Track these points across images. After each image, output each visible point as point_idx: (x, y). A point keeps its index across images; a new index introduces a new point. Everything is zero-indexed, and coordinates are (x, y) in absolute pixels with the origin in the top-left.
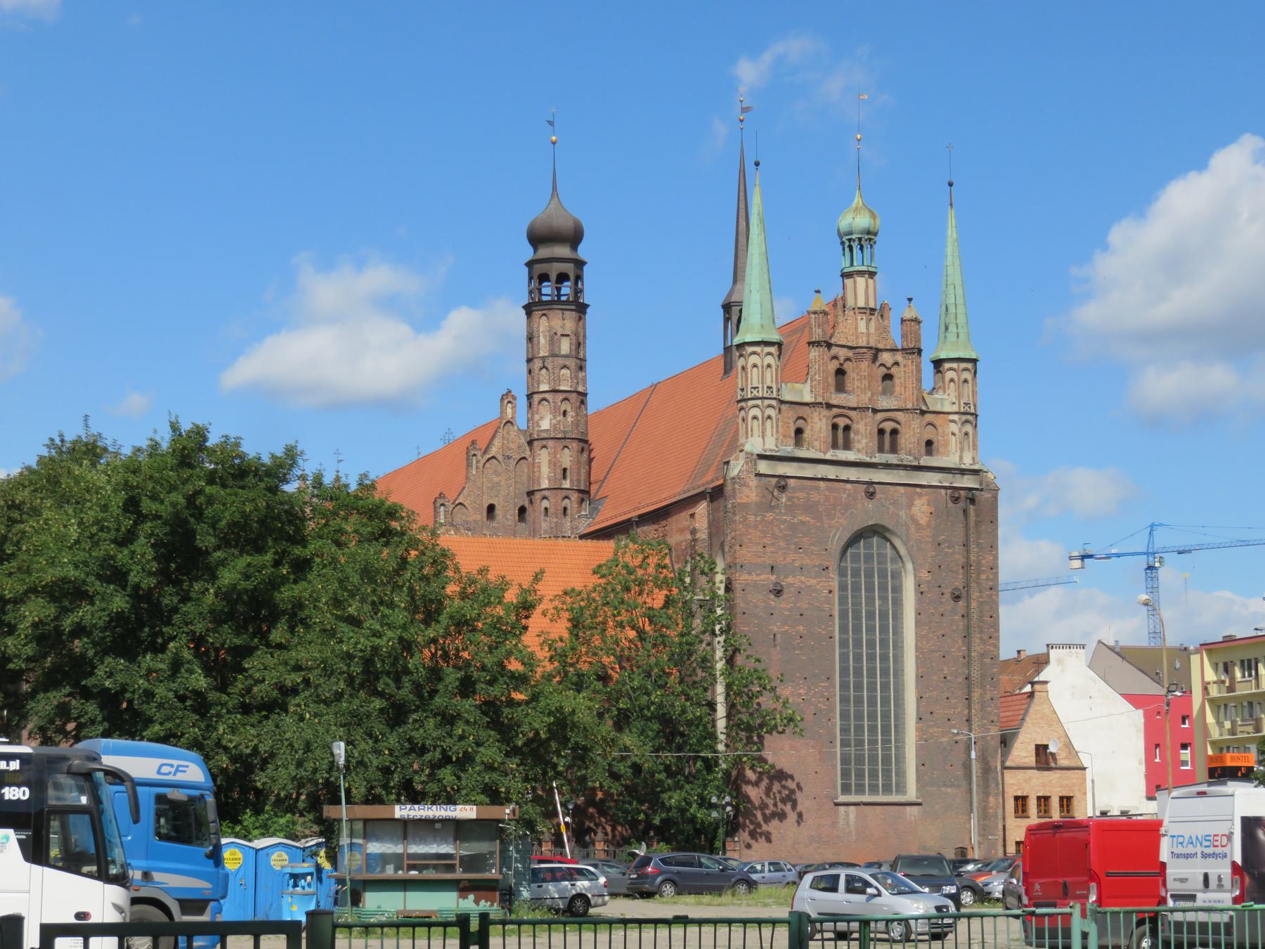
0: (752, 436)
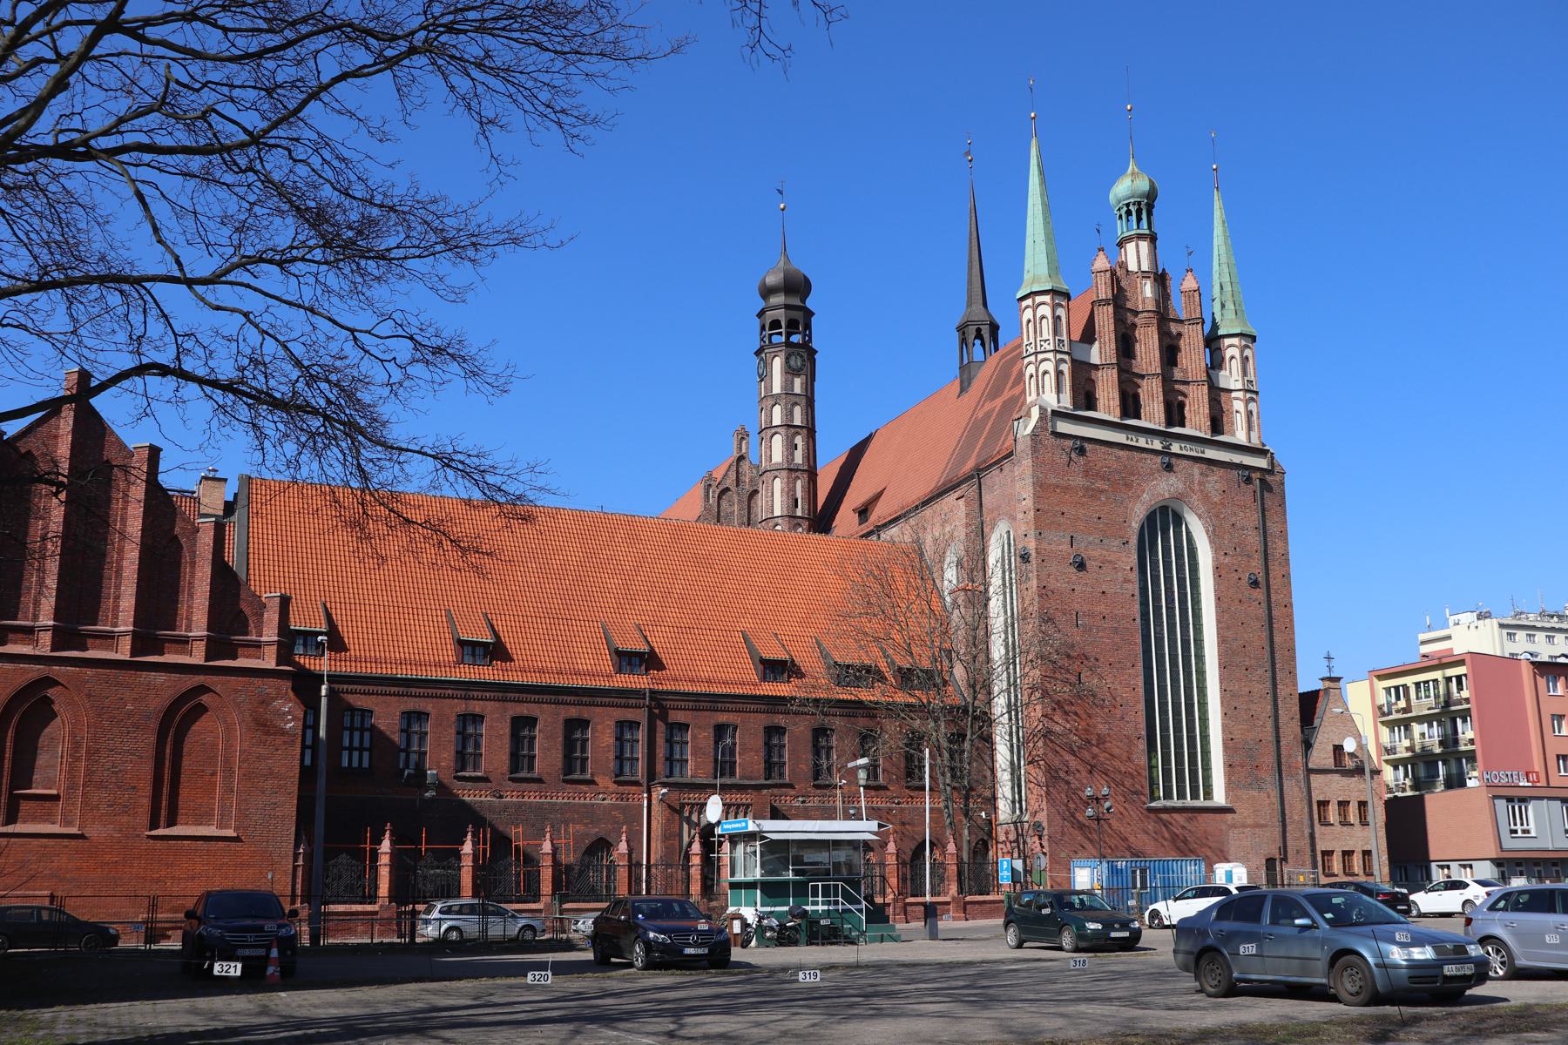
0: (1044, 392)
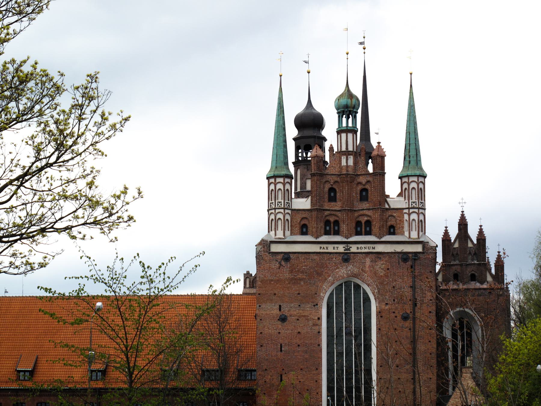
0: (271, 230)
